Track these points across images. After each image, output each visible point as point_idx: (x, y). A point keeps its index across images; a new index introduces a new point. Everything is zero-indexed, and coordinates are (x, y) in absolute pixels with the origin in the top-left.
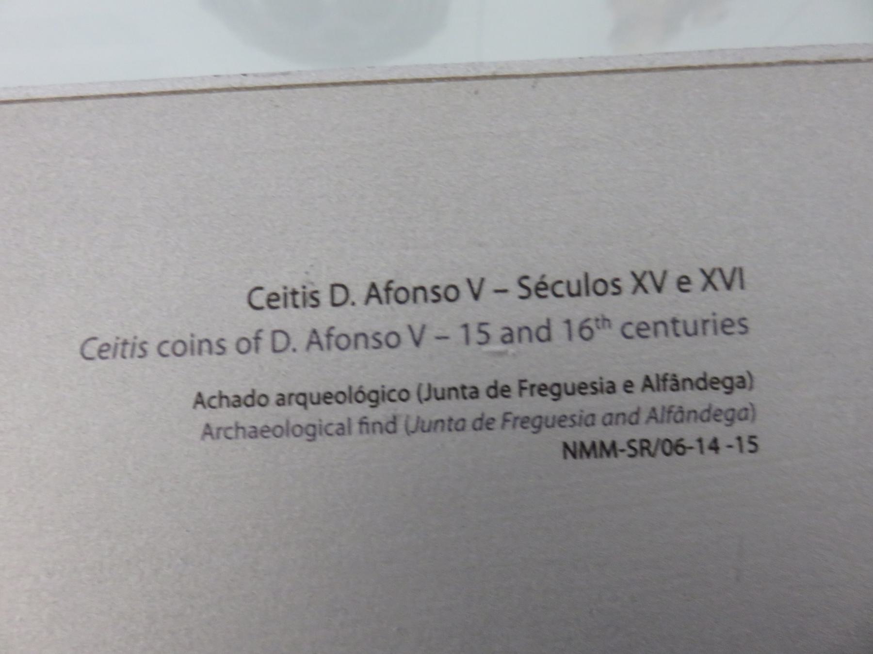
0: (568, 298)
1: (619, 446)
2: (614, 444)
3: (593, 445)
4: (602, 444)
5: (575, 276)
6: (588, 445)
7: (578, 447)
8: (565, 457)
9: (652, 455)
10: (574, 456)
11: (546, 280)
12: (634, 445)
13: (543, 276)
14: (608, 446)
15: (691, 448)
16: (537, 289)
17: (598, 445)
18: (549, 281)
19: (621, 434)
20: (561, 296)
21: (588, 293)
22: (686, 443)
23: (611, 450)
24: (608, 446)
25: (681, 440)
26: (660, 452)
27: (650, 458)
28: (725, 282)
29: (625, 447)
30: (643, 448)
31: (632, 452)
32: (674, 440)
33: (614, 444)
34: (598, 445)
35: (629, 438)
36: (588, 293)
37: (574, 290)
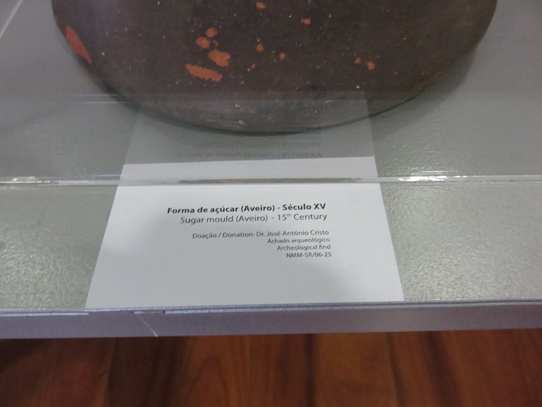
1: (302, 255)
2: (301, 254)
3: (295, 254)
5: (301, 204)
6: (294, 254)
13: (291, 205)
14: (300, 254)
16: (289, 208)
17: (297, 254)
18: (293, 206)
20: (296, 209)
28: (322, 206)
34: (297, 254)
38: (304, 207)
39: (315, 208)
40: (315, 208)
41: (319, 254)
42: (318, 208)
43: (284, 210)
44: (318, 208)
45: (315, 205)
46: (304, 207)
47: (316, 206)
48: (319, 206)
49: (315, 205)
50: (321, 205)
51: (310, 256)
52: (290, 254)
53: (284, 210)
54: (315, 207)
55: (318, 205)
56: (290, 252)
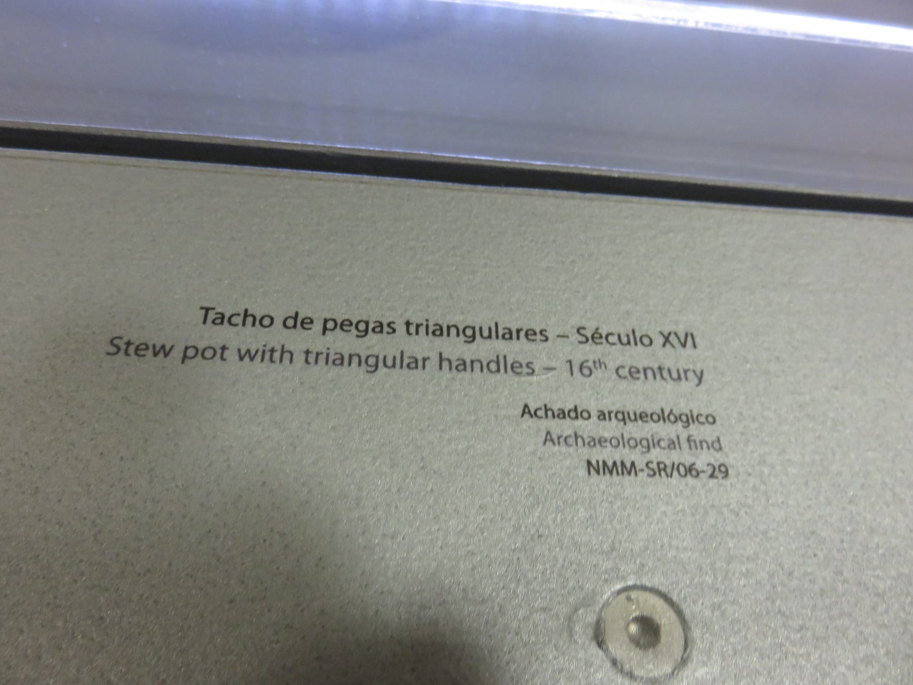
0: (619, 346)
2: (633, 464)
3: (615, 464)
4: (623, 464)
6: (610, 464)
7: (601, 464)
8: (589, 473)
10: (598, 472)
11: (600, 331)
14: (628, 465)
15: (703, 472)
16: (593, 337)
17: (619, 464)
21: (636, 344)
23: (631, 469)
24: (628, 465)
25: (694, 464)
26: (675, 473)
29: (644, 466)
30: (661, 469)
32: (687, 464)
34: (619, 464)
36: (636, 344)
37: (625, 340)
38: (634, 339)
39: (664, 345)
40: (664, 345)
41: (690, 470)
42: (673, 346)
43: (580, 342)
44: (673, 346)
45: (661, 333)
46: (634, 339)
47: (667, 340)
48: (673, 338)
49: (661, 333)
50: (676, 334)
51: (663, 473)
52: (598, 462)
53: (580, 342)
54: (661, 340)
55: (669, 334)
56: (599, 455)
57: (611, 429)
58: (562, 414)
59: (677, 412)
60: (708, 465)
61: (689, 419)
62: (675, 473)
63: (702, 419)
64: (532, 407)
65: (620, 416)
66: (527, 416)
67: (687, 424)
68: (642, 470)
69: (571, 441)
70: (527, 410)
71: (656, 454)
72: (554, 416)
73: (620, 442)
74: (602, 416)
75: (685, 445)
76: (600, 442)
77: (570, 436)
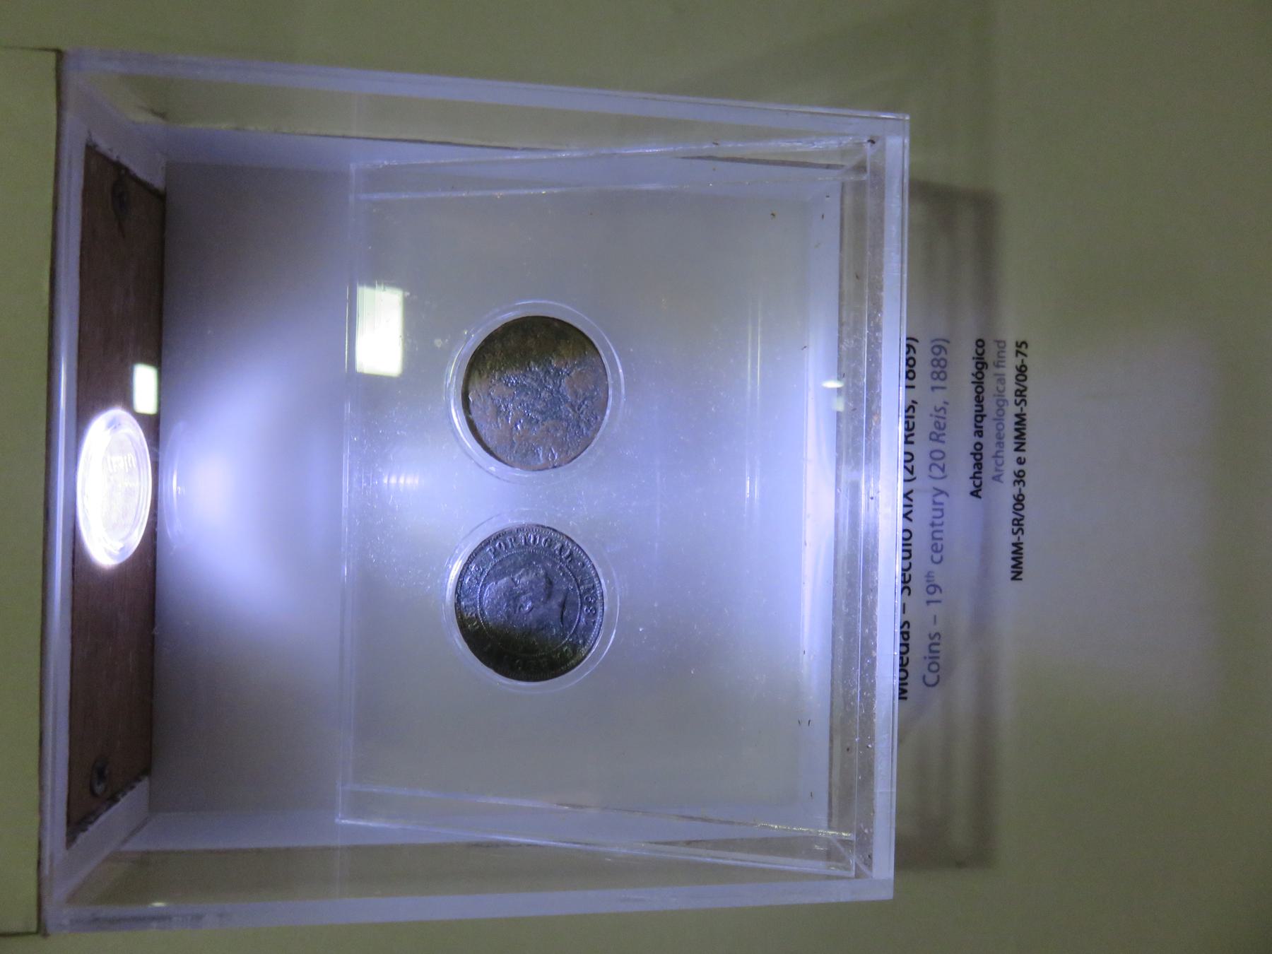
4: (1017, 423)
6: (1017, 434)
7: (1017, 441)
9: (1026, 389)
12: (1018, 402)
15: (1022, 361)
17: (1017, 427)
19: (1011, 410)
22: (1019, 364)
24: (1017, 420)
27: (1028, 390)
31: (1023, 403)
33: (1017, 415)
34: (1017, 427)
35: (1014, 405)
57: (988, 425)
58: (978, 465)
59: (975, 371)
60: (1017, 355)
61: (981, 364)
62: (1025, 383)
63: (980, 351)
64: (973, 489)
65: (979, 419)
66: (980, 493)
67: (985, 364)
68: (1022, 409)
69: (1000, 461)
70: (975, 494)
71: (1010, 395)
72: (980, 473)
73: (999, 419)
74: (979, 432)
75: (1000, 371)
76: (1000, 438)
77: (996, 462)
